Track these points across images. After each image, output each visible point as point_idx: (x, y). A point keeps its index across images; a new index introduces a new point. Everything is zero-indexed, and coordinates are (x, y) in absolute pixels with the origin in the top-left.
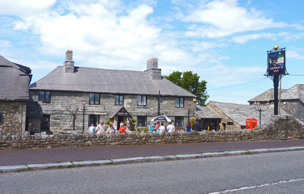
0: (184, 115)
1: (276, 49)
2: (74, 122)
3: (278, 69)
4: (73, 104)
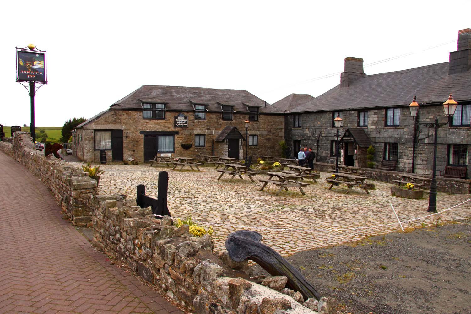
0: (467, 141)
1: (31, 49)
3: (34, 75)
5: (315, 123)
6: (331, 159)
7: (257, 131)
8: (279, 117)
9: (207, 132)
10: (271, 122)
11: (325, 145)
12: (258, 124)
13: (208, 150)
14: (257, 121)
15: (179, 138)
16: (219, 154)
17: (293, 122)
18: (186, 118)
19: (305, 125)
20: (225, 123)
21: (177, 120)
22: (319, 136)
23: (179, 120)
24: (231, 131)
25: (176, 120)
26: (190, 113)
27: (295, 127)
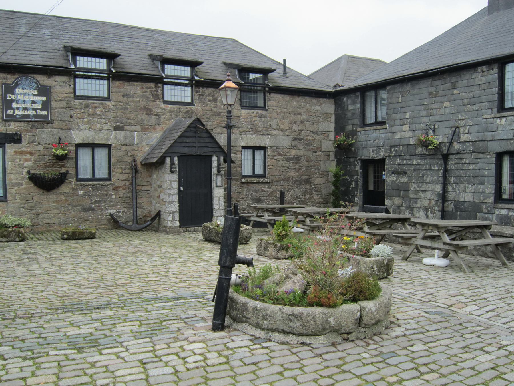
2: (445, 185)
4: (444, 118)
5: (434, 106)
6: (497, 212)
7: (265, 137)
8: (322, 100)
9: (115, 138)
10: (300, 114)
11: (471, 167)
12: (265, 117)
13: (121, 191)
14: (264, 108)
15: (22, 153)
16: (154, 202)
17: (358, 111)
18: (43, 91)
19: (398, 116)
20: (170, 111)
21: (12, 97)
22: (451, 143)
23: (20, 98)
24: (185, 131)
25: (10, 97)
26: (58, 78)
27: (364, 124)
